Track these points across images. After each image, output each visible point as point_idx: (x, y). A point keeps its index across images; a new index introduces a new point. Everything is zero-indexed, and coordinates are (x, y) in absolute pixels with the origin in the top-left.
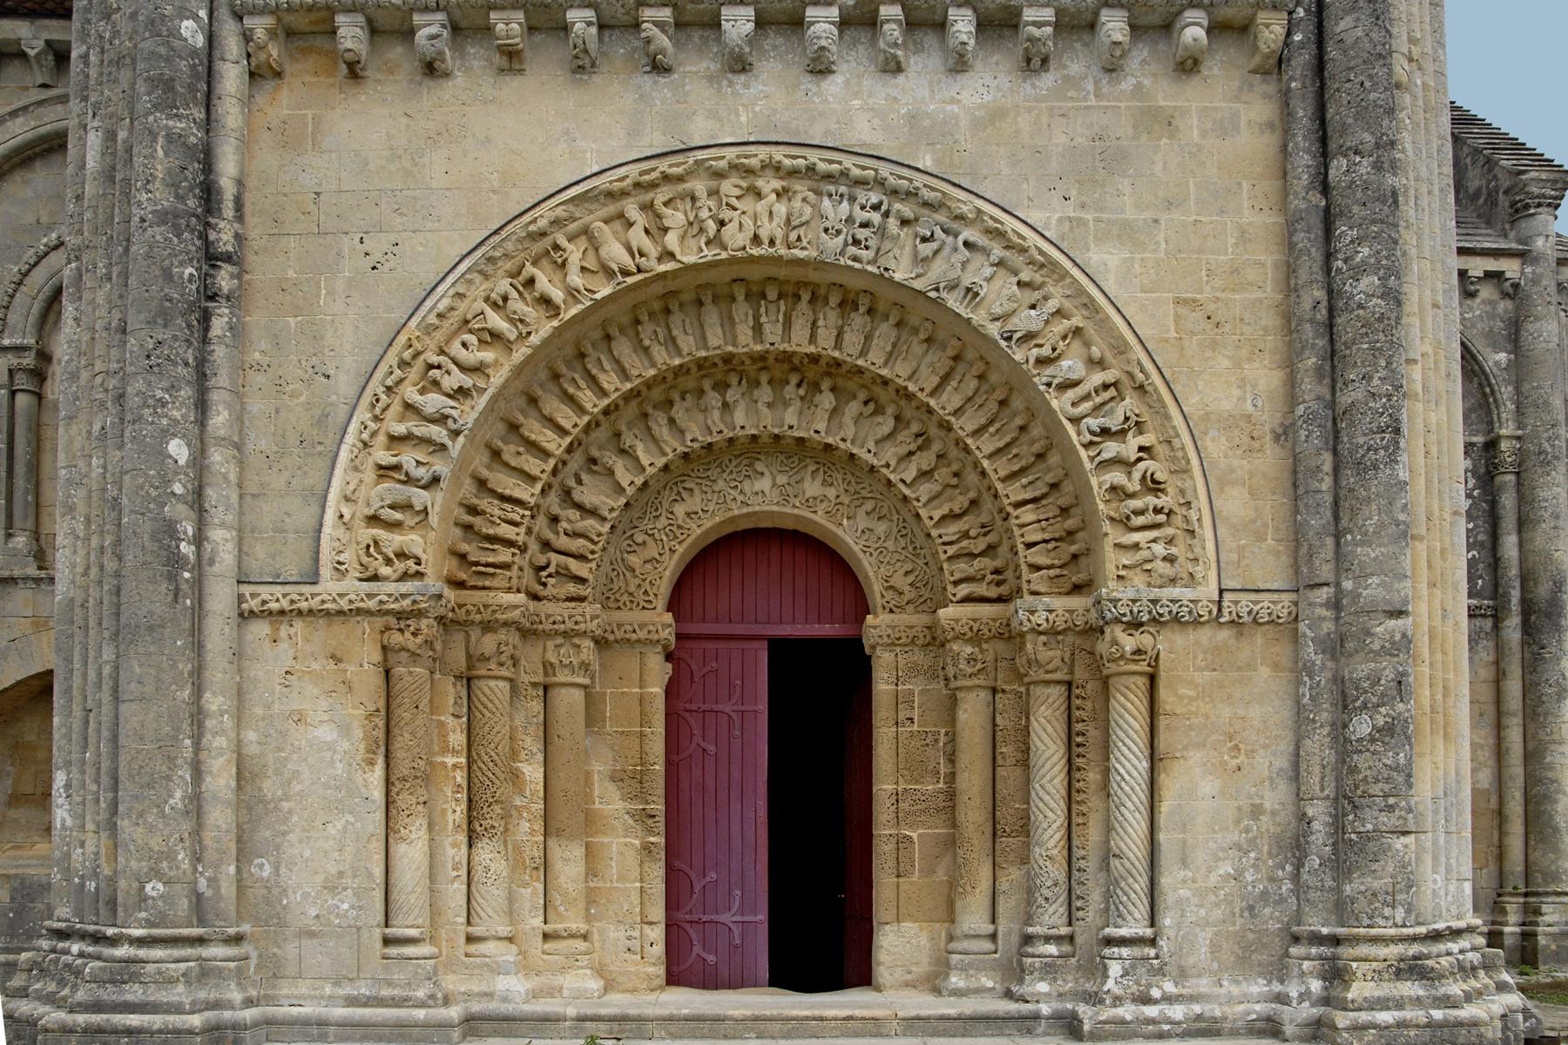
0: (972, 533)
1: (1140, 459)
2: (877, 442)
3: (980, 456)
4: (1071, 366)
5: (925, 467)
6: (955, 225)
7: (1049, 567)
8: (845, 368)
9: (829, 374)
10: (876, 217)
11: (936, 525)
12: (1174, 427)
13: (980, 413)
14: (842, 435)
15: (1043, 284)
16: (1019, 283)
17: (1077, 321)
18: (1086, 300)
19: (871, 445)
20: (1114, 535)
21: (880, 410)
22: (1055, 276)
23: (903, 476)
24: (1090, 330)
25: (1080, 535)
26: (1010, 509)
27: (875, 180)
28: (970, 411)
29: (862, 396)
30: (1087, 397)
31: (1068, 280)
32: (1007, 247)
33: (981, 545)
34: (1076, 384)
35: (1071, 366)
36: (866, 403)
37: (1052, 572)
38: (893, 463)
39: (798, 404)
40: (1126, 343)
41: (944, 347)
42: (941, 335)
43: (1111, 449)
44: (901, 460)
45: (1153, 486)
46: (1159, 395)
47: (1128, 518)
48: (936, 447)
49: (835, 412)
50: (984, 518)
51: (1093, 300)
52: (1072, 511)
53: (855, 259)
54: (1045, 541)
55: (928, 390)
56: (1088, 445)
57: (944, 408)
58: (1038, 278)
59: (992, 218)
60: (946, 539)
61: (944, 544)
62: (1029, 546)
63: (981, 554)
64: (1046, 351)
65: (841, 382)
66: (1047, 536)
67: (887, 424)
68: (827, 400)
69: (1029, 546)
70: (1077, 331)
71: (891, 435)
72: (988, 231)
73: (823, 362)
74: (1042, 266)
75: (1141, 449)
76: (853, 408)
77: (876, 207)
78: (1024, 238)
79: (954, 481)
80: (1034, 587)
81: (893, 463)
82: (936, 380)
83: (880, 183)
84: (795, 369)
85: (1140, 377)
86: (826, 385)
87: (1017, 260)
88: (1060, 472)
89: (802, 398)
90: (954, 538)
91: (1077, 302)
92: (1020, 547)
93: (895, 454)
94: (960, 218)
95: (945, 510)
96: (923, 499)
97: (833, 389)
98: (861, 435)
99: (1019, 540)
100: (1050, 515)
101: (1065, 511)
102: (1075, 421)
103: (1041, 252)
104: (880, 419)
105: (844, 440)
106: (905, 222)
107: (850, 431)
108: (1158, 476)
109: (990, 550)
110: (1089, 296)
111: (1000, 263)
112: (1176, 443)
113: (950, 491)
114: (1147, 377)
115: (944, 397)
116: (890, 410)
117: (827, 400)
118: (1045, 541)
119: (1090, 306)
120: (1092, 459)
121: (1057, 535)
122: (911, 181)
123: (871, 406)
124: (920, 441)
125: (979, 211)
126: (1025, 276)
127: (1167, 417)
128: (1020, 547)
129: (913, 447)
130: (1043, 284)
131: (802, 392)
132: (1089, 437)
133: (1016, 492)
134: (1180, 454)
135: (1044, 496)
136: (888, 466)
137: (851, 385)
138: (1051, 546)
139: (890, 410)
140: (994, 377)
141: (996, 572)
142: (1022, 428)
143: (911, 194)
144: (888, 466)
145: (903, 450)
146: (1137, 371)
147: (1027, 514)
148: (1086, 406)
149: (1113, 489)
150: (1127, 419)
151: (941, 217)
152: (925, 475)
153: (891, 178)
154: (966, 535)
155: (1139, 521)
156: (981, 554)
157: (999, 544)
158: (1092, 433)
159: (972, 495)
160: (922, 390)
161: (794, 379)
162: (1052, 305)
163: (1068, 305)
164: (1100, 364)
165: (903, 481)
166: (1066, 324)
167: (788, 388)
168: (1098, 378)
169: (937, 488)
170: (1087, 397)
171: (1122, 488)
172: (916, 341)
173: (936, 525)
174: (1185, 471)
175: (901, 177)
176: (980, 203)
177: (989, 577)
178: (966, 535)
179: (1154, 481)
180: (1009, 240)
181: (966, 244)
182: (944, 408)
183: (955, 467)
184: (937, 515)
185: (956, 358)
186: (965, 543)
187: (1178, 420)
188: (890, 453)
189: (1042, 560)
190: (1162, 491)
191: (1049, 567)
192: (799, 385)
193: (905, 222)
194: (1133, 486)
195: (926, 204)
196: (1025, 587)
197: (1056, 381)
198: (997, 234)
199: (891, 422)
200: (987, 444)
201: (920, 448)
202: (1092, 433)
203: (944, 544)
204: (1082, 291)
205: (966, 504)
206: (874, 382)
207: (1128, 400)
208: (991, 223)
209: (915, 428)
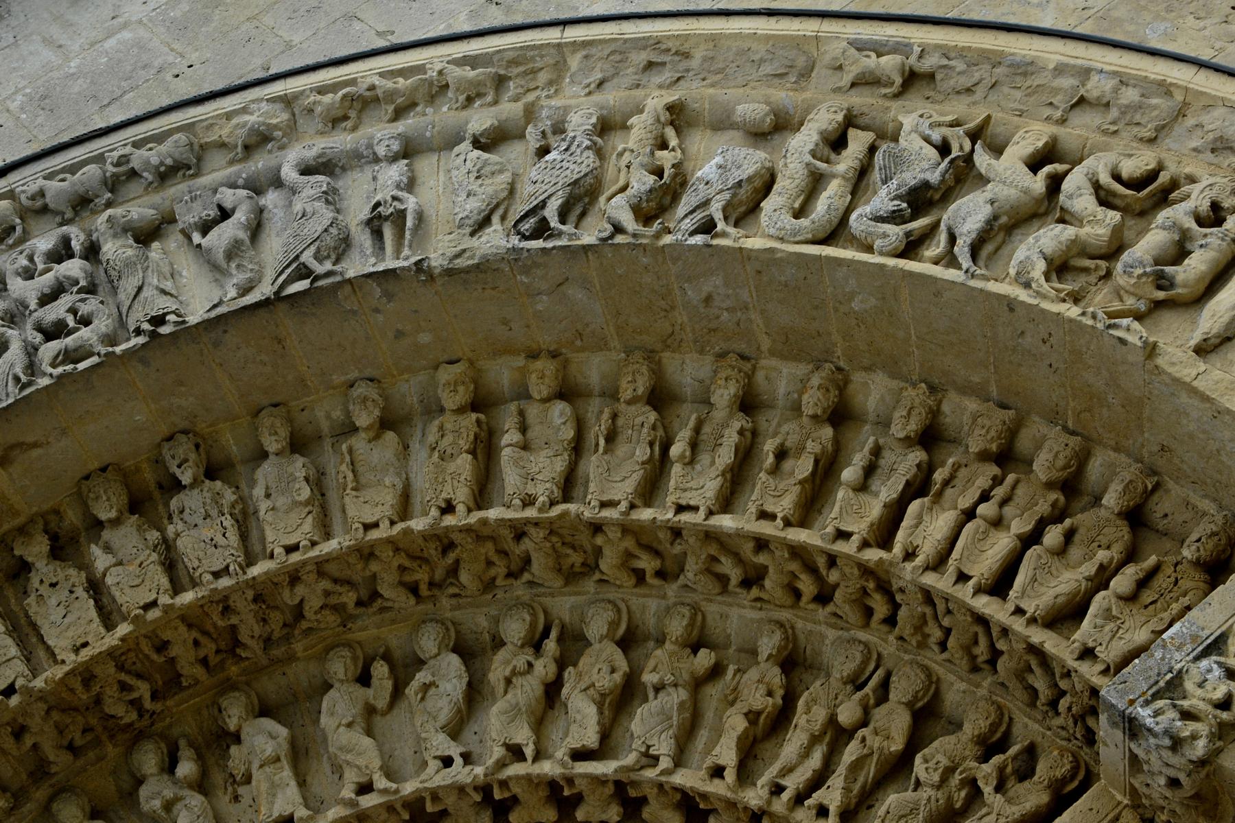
0: (847, 714)
1: (1055, 183)
2: (454, 732)
3: (698, 518)
4: (717, 164)
5: (607, 681)
6: (260, 163)
7: (1101, 580)
8: (249, 628)
9: (229, 686)
10: (74, 268)
11: (745, 774)
12: (1060, 70)
13: (622, 449)
14: (352, 778)
15: (530, 114)
16: (477, 144)
17: (656, 101)
18: (643, 57)
19: (442, 744)
20: (1176, 340)
21: (405, 667)
22: (543, 77)
23: (574, 742)
24: (694, 92)
25: (1095, 468)
26: (873, 555)
27: (24, 213)
28: (592, 465)
29: (339, 666)
30: (816, 182)
31: (574, 62)
32: (398, 114)
33: (894, 724)
34: (766, 183)
35: (717, 164)
36: (364, 679)
37: (1123, 582)
38: (523, 735)
39: (196, 800)
40: (798, 42)
41: (434, 409)
42: (408, 390)
43: (969, 213)
44: (539, 725)
45: (1148, 193)
46: (962, 52)
47: (1163, 282)
48: (596, 627)
49: (300, 755)
50: (843, 665)
51: (655, 43)
52: (1024, 443)
53: (71, 356)
54: (1032, 539)
55: (461, 495)
56: (911, 248)
57: (528, 501)
58: (509, 109)
59: (322, 90)
60: (793, 783)
61: (799, 799)
62: (1000, 585)
63: (914, 744)
64: (642, 182)
65: (271, 686)
66: (1020, 525)
67: (449, 676)
68: (264, 739)
69: (1000, 585)
70: (678, 116)
71: (475, 695)
72: (336, 121)
73: (182, 651)
74: (500, 82)
75: (1035, 164)
76: (337, 711)
77: (62, 253)
78: (420, 69)
79: (705, 659)
80: (1110, 653)
81: (523, 735)
82: (464, 464)
83: (39, 209)
84: (139, 737)
85: (889, 63)
86: (234, 714)
87: (442, 116)
88: (916, 395)
89: (202, 785)
90: (816, 760)
91: (629, 74)
92: (984, 604)
93: (514, 713)
94: (259, 140)
95: (736, 724)
96: (664, 747)
97: (265, 711)
98: (404, 752)
99: (965, 593)
100: (982, 482)
101: (1005, 457)
102: (836, 233)
103: (471, 61)
104: (422, 677)
105: (365, 788)
106: (146, 236)
107: (362, 754)
108: (1130, 168)
109: (927, 717)
110: (642, 43)
111: (408, 151)
112: (1096, 87)
113: (713, 692)
114: (901, 48)
115: (510, 478)
116: (428, 642)
117: (264, 739)
118: (1032, 539)
119: (658, 59)
120: (949, 259)
121: (1043, 508)
122: (100, 159)
123: (380, 670)
124: (551, 645)
125: (287, 101)
126: (480, 120)
127: (1024, 69)
128: (984, 604)
129: (544, 668)
130: (530, 114)
131: (186, 768)
132: (895, 232)
133: (853, 512)
134: (1130, 95)
135: (926, 471)
136: (516, 753)
137: (301, 673)
138: (1053, 536)
139: (428, 642)
140: (593, 369)
141: (989, 747)
142: (748, 404)
143: (121, 180)
144: (516, 753)
145: (529, 689)
146: (871, 62)
147: (928, 527)
148: (831, 197)
149: (1059, 268)
150: (944, 149)
151: (217, 171)
152: (625, 697)
153: (54, 186)
154: (836, 735)
155: (1197, 264)
156: (914, 744)
157: (934, 686)
158: (895, 218)
159: (768, 644)
160: (448, 508)
161: (149, 760)
162: (580, 122)
163: (612, 97)
164: (781, 125)
165: (580, 755)
166: (641, 125)
167: (144, 792)
168: (803, 142)
169: (675, 697)
170: (816, 182)
171: (1079, 248)
172: (359, 443)
173: (745, 774)
174: (1181, 113)
175: (73, 169)
176: (277, 88)
177: (986, 772)
178: (836, 735)
179: (1137, 184)
180: (391, 95)
181: (306, 171)
182: (528, 501)
183: (676, 627)
184: (727, 754)
185: (480, 403)
186: (851, 752)
187: (1052, 52)
188: (501, 724)
189: (1066, 581)
190: (1174, 185)
191: (1101, 580)
192: (170, 766)
193: (146, 236)
194: (1099, 224)
195: (167, 174)
196: (1089, 672)
197: (716, 210)
198: (361, 104)
199: (454, 662)
200: (697, 485)
201: (562, 664)
202: (895, 218)
203: (799, 799)
204: (622, 49)
205: (775, 676)
206: (346, 619)
207: (908, 121)
208: (328, 99)
209: (515, 629)
